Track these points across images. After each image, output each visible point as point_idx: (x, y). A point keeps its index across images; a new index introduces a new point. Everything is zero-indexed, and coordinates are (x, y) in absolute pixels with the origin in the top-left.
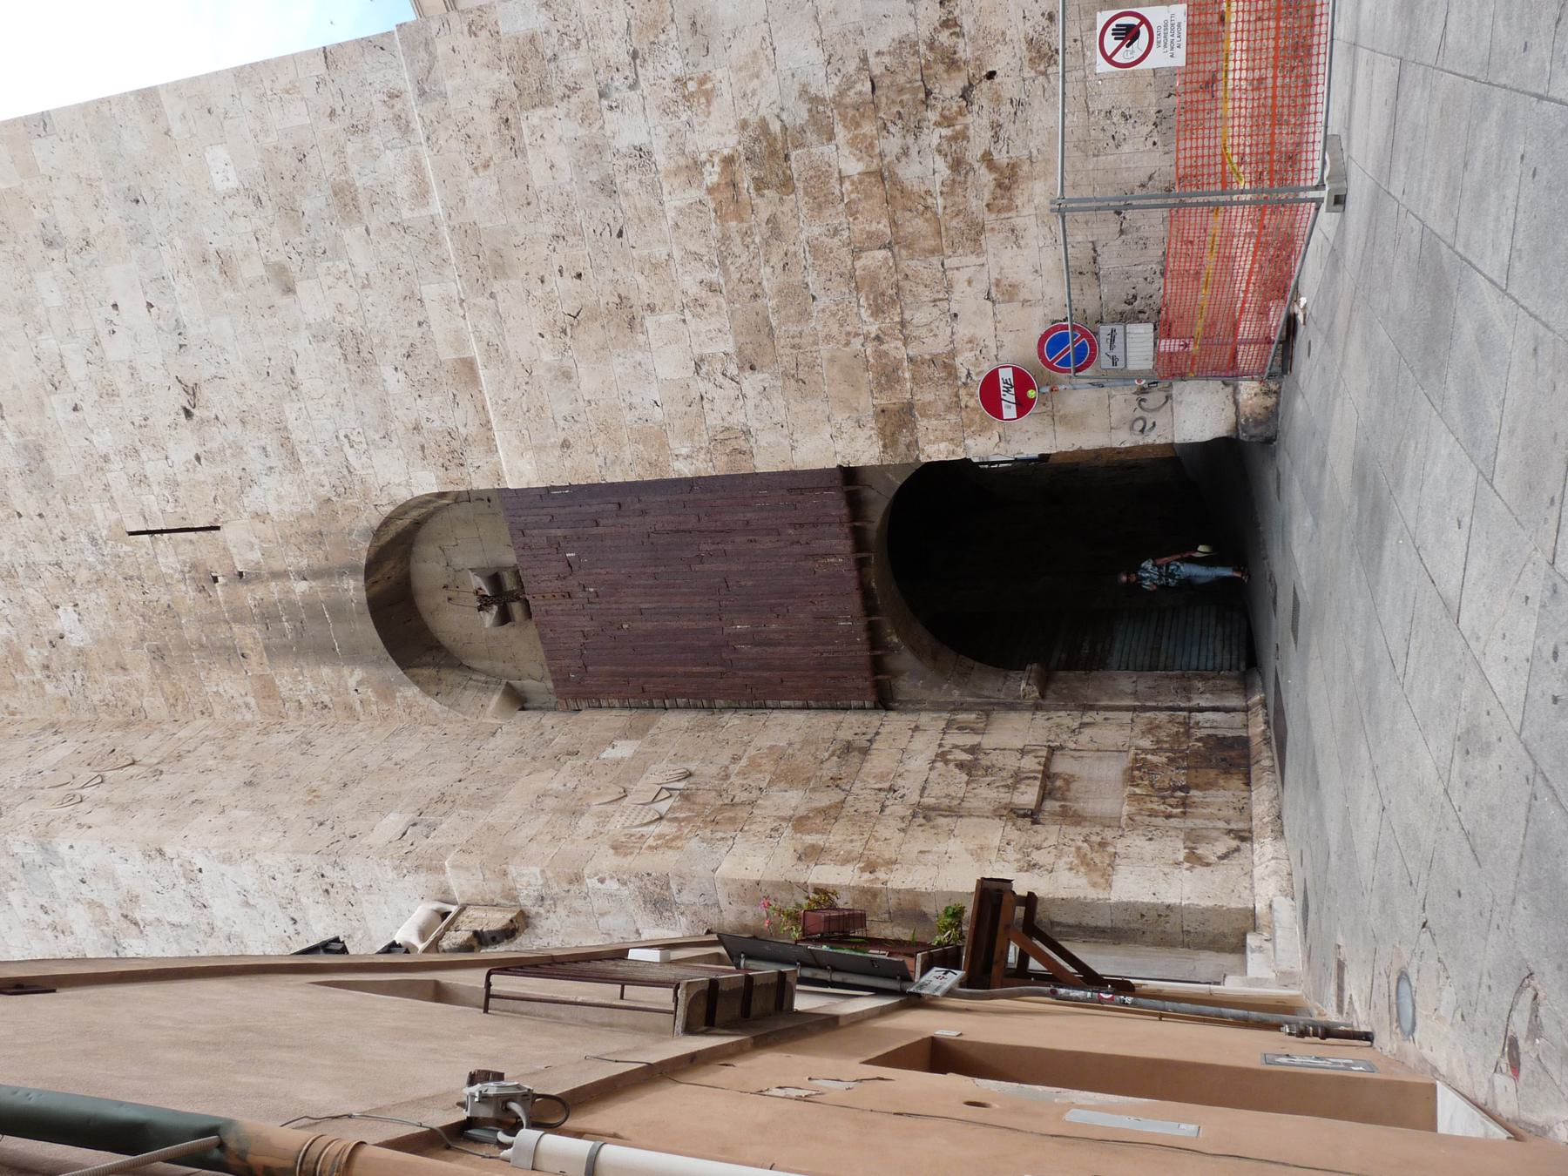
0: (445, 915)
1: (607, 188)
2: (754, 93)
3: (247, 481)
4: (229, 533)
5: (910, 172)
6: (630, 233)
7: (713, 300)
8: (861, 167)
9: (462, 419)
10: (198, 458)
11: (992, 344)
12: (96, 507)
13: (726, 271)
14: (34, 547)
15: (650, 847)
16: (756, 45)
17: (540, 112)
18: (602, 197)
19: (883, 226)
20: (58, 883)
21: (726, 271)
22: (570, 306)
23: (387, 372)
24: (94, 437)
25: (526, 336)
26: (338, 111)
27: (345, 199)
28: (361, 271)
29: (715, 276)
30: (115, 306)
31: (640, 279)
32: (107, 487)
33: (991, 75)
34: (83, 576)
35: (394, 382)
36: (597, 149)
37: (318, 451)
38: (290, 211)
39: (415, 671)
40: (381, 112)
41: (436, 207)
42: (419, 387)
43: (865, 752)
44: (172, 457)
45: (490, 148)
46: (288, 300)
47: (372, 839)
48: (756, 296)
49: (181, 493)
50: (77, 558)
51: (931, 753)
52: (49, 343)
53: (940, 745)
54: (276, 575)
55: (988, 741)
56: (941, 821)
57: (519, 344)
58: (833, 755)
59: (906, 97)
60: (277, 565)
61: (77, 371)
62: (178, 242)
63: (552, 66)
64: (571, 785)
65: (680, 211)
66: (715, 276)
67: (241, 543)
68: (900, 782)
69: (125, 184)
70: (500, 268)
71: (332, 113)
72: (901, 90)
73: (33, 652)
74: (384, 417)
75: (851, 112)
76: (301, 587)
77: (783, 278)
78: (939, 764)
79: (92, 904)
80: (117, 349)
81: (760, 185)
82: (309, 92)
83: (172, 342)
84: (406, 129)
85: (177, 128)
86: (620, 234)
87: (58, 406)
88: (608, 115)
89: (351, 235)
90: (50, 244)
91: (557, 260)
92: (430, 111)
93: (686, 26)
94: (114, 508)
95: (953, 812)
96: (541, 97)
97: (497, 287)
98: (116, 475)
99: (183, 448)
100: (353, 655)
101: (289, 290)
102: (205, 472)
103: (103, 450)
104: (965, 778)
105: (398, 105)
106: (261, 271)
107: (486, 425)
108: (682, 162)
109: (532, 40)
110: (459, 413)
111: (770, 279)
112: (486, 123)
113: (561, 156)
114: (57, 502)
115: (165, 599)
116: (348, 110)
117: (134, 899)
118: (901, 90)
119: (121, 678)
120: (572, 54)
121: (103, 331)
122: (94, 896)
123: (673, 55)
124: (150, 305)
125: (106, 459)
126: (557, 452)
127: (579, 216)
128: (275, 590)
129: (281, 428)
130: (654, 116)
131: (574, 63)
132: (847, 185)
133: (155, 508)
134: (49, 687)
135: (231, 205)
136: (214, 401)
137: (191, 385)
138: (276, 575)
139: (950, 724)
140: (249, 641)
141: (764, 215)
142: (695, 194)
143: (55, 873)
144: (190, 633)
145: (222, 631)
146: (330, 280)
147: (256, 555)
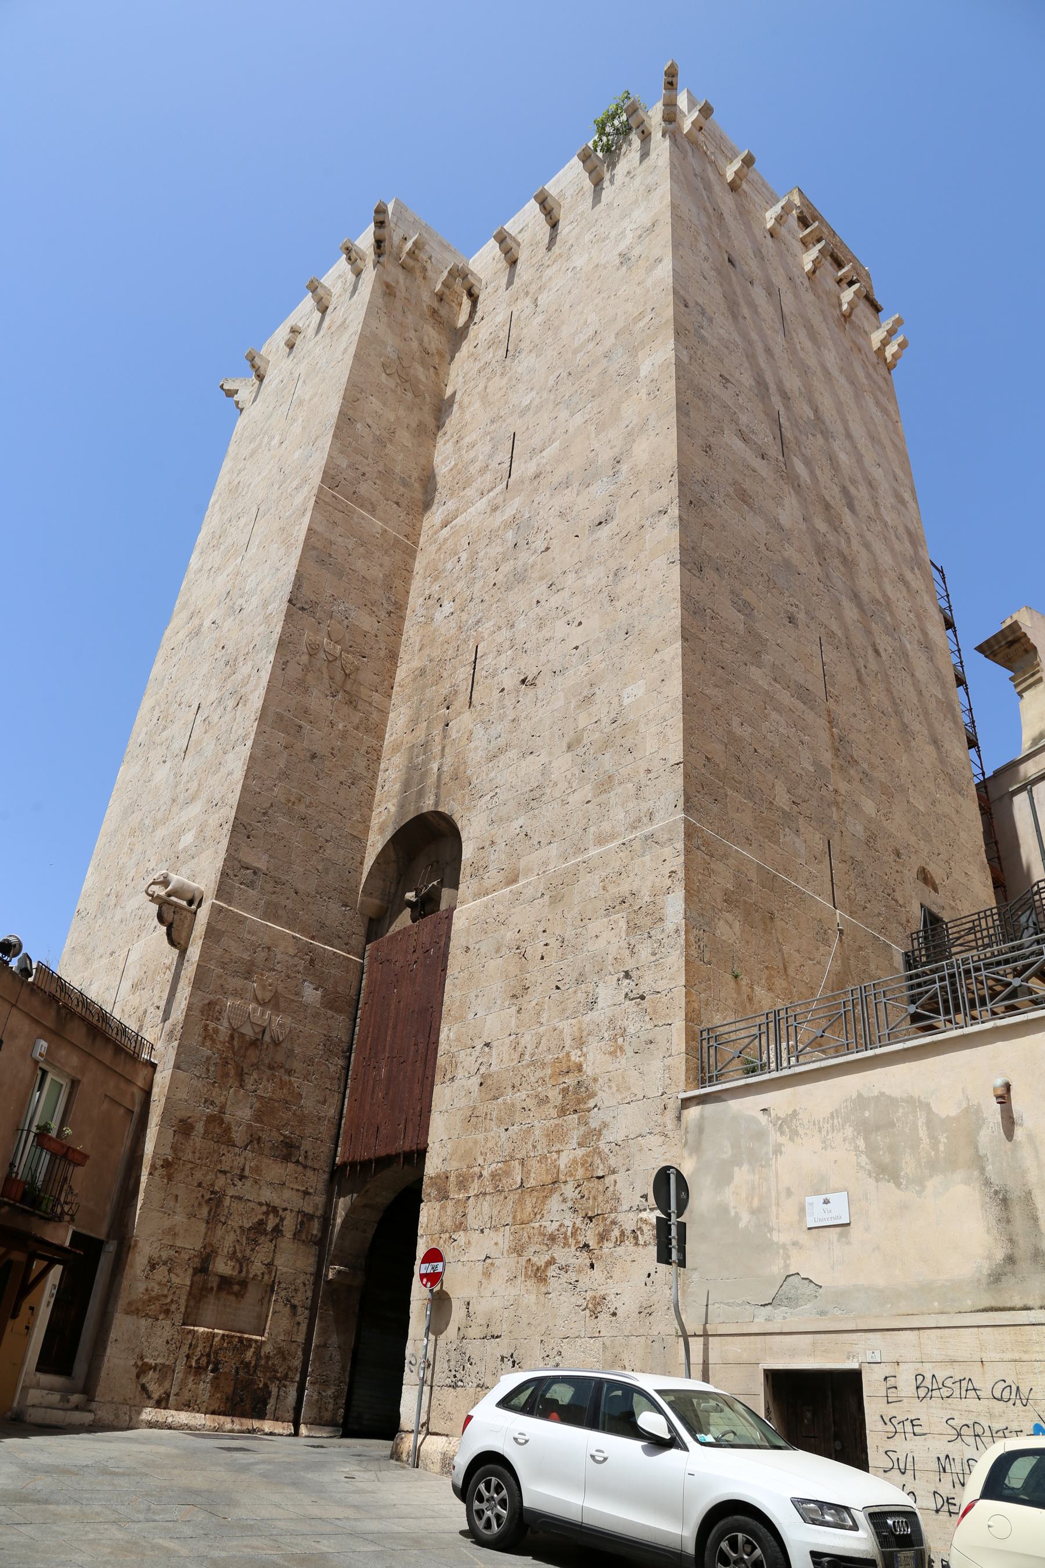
2: (610, 1087)
5: (554, 1203)
7: (516, 1056)
8: (562, 1167)
11: (465, 1259)
13: (528, 1066)
15: (207, 1026)
16: (633, 1090)
17: (624, 928)
18: (576, 975)
19: (531, 1183)
21: (528, 1066)
26: (650, 776)
28: (570, 799)
31: (534, 1003)
33: (592, 1266)
37: (492, 775)
38: (606, 744)
39: (391, 847)
40: (644, 806)
43: (286, 1158)
45: (613, 890)
46: (565, 748)
51: (277, 1202)
53: (285, 1209)
55: (286, 1243)
56: (205, 1211)
58: (285, 1136)
59: (591, 1201)
61: (556, 600)
63: (646, 935)
64: (278, 967)
68: (249, 1183)
69: (636, 624)
71: (649, 771)
73: (437, 588)
75: (589, 1160)
76: (435, 766)
77: (519, 1107)
78: (264, 1208)
86: (558, 988)
87: (540, 590)
91: (552, 941)
92: (637, 846)
93: (650, 1037)
96: (633, 927)
99: (509, 680)
100: (402, 806)
104: (247, 1225)
105: (645, 820)
108: (585, 1034)
112: (624, 888)
116: (649, 783)
118: (595, 1198)
120: (650, 950)
121: (569, 617)
123: (638, 1025)
124: (576, 648)
126: (465, 944)
130: (609, 1013)
131: (644, 952)
132: (555, 1156)
133: (486, 663)
136: (528, 695)
137: (537, 682)
139: (305, 1215)
142: (568, 1042)
146: (569, 776)
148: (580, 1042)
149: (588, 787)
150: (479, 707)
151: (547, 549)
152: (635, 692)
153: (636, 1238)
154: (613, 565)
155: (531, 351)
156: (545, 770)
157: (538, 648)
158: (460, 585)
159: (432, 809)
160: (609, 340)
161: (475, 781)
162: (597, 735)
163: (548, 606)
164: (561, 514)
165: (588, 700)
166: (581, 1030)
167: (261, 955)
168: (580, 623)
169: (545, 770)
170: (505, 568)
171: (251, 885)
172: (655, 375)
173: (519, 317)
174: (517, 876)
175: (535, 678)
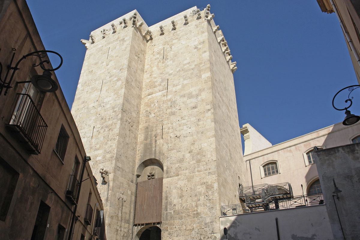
0: (107, 173)
1: (196, 196)
3: (167, 143)
4: (161, 140)
5: (193, 232)
6: (191, 198)
7: (182, 207)
8: (194, 227)
9: (172, 174)
10: (171, 137)
12: (166, 122)
14: (162, 112)
17: (205, 188)
20: (115, 120)
22: (183, 189)
23: (178, 165)
24: (175, 123)
25: (181, 183)
27: (199, 161)
28: (191, 162)
29: (185, 208)
30: (190, 128)
31: (185, 199)
32: (169, 124)
34: (158, 118)
35: (177, 165)
36: (200, 195)
38: (198, 154)
40: (208, 167)
41: (197, 173)
42: (176, 168)
44: (171, 134)
45: (202, 181)
46: (188, 152)
47: (118, 163)
48: (182, 213)
49: (167, 134)
50: (161, 118)
52: (186, 118)
54: (156, 146)
57: (180, 182)
60: (157, 146)
61: (183, 121)
62: (196, 138)
65: (192, 204)
66: (185, 208)
67: (160, 141)
70: (188, 181)
71: (209, 161)
72: (202, 232)
74: (173, 163)
79: (112, 124)
80: (185, 127)
81: (194, 214)
82: (212, 158)
83: (185, 135)
84: (206, 170)
85: (209, 140)
87: (179, 118)
88: (204, 196)
89: (194, 162)
90: (198, 120)
91: (189, 188)
92: (207, 174)
93: (212, 207)
94: (166, 124)
95: (117, 234)
96: (207, 188)
97: (186, 180)
98: (170, 125)
101: (189, 152)
102: (169, 138)
103: (173, 124)
106: (192, 149)
107: (171, 177)
109: (213, 187)
110: (173, 173)
111: (184, 215)
112: (205, 181)
113: (200, 190)
114: (167, 116)
115: (154, 130)
117: (112, 130)
119: (145, 122)
122: (113, 125)
123: (209, 205)
125: (172, 124)
127: (193, 191)
128: (154, 146)
129: (173, 149)
131: (210, 193)
134: (144, 111)
135: (200, 146)
138: (156, 146)
140: (148, 141)
141: (191, 215)
142: (194, 206)
143: (116, 120)
144: (150, 133)
145: (149, 138)
146: (190, 158)
147: (158, 144)
148: (197, 206)
149: (195, 161)
150: (165, 139)
151: (180, 109)
152: (205, 145)
153: (211, 238)
154: (198, 118)
155: (171, 60)
156: (184, 156)
157: (180, 131)
158: (156, 111)
159: (153, 158)
160: (193, 66)
161: (165, 154)
162: (196, 151)
163: (181, 122)
164: (183, 103)
165: (193, 144)
166: (197, 204)
167: (121, 184)
168: (190, 128)
169: (184, 156)
170: (169, 111)
171: (119, 170)
172: (206, 79)
173: (166, 50)
174: (179, 175)
175: (179, 137)
